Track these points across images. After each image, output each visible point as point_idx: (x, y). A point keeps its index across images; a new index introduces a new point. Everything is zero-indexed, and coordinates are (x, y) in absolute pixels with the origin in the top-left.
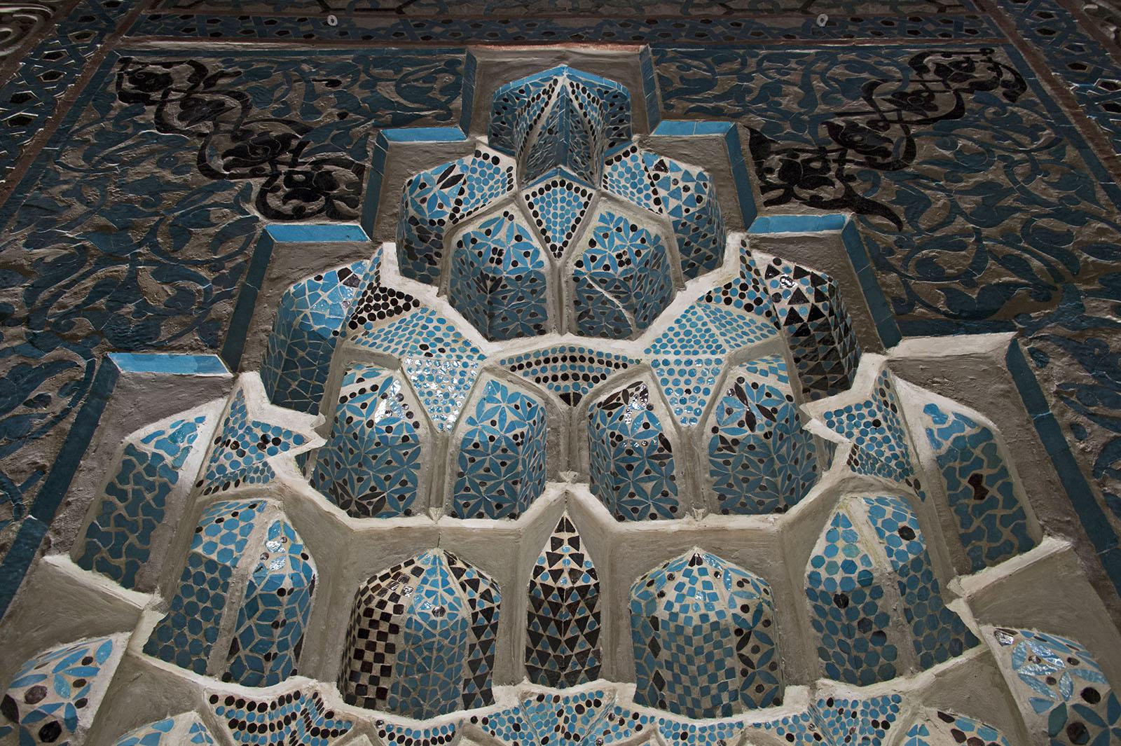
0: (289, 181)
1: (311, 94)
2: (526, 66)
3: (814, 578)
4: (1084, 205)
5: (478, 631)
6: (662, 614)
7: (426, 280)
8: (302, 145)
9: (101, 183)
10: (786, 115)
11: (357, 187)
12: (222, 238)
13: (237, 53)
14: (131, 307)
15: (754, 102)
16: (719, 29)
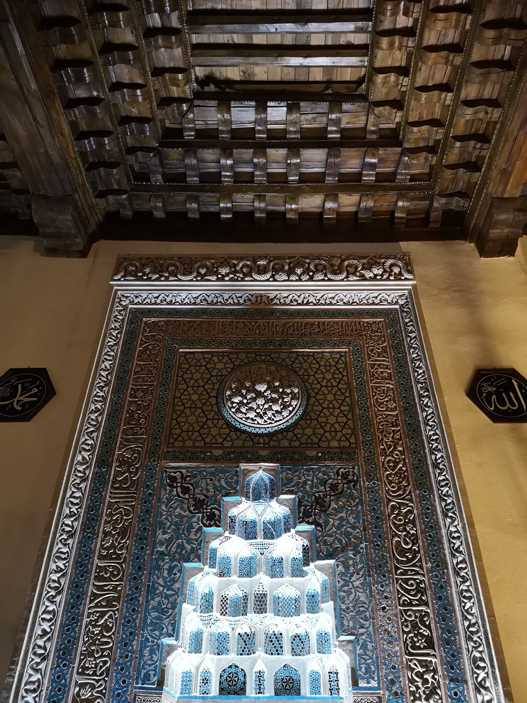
0: (206, 515)
1: (207, 485)
2: (253, 470)
3: (308, 592)
4: (357, 524)
5: (244, 600)
6: (280, 596)
7: (233, 534)
8: (208, 502)
9: (170, 515)
10: (307, 492)
11: (219, 516)
12: (196, 532)
13: (189, 468)
14: (184, 551)
15: (301, 487)
16: (296, 456)
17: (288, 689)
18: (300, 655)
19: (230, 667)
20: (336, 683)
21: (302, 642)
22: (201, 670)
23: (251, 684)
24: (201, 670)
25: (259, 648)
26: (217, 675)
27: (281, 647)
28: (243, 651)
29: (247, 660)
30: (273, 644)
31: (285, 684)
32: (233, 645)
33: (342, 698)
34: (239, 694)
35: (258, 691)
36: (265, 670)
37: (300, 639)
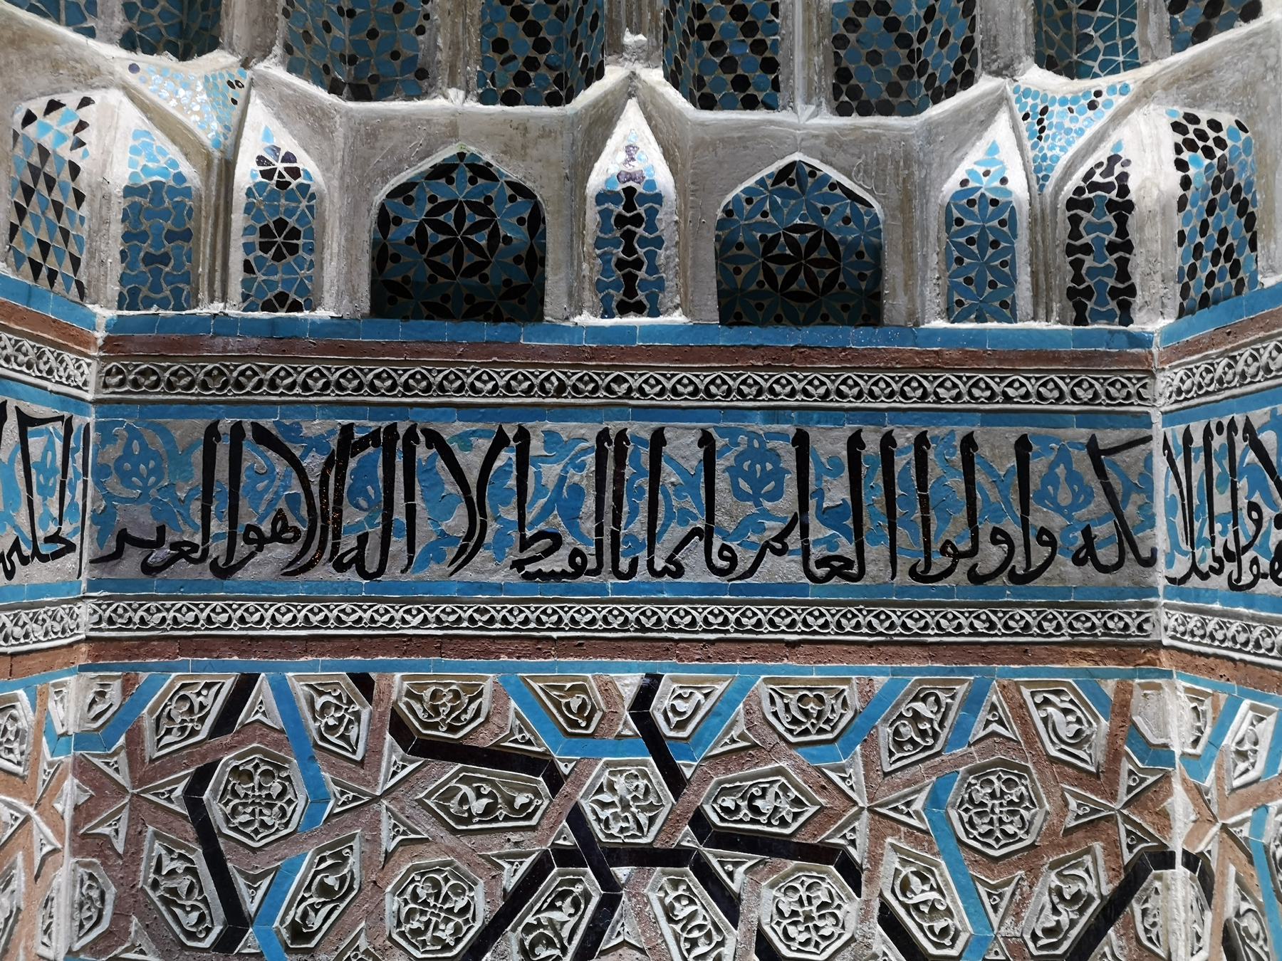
17: (801, 297)
18: (886, 110)
19: (443, 171)
20: (1111, 260)
21: (904, 41)
22: (246, 173)
23: (573, 260)
24: (246, 173)
25: (629, 38)
26: (355, 208)
27: (770, 66)
28: (521, 79)
29: (547, 132)
30: (717, 48)
31: (781, 271)
32: (455, 46)
33: (1142, 341)
34: (497, 318)
35: (618, 296)
36: (664, 179)
37: (892, 25)
